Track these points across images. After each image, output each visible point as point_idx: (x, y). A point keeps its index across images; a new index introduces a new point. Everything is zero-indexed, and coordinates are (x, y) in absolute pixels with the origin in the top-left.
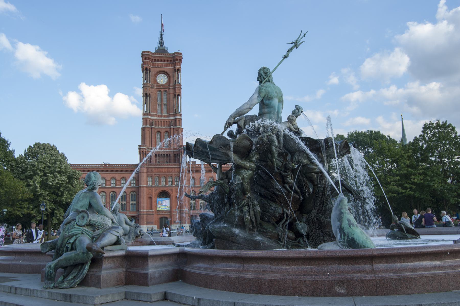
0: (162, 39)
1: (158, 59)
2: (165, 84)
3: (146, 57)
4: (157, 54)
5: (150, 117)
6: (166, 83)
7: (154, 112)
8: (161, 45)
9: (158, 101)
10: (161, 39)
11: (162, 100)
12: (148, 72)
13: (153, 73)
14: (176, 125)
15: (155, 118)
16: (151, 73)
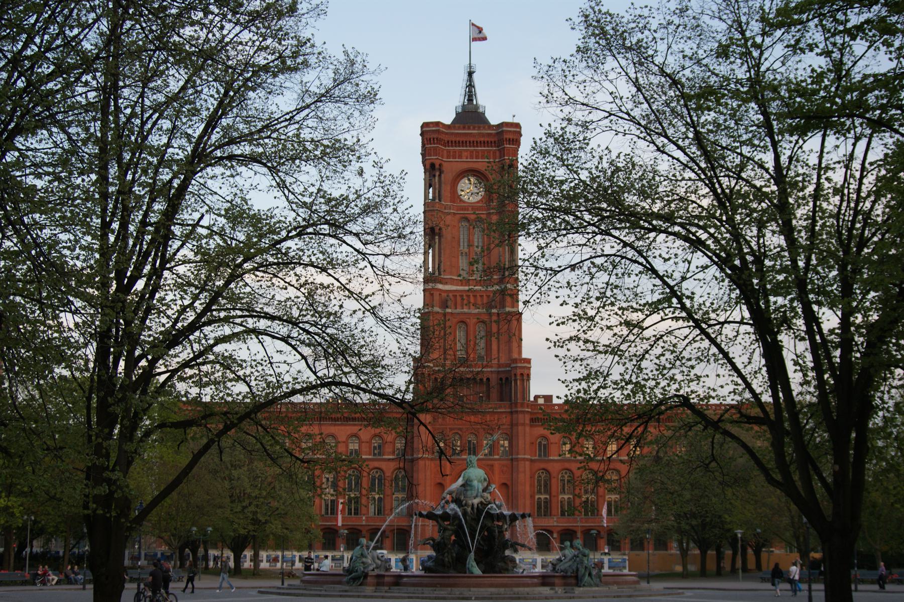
0: (470, 86)
1: (461, 140)
2: (478, 202)
3: (432, 136)
4: (459, 128)
5: (440, 286)
6: (481, 200)
7: (451, 274)
8: (470, 100)
9: (461, 244)
10: (470, 85)
11: (470, 245)
12: (437, 174)
13: (448, 176)
14: (504, 307)
15: (454, 288)
16: (443, 175)
